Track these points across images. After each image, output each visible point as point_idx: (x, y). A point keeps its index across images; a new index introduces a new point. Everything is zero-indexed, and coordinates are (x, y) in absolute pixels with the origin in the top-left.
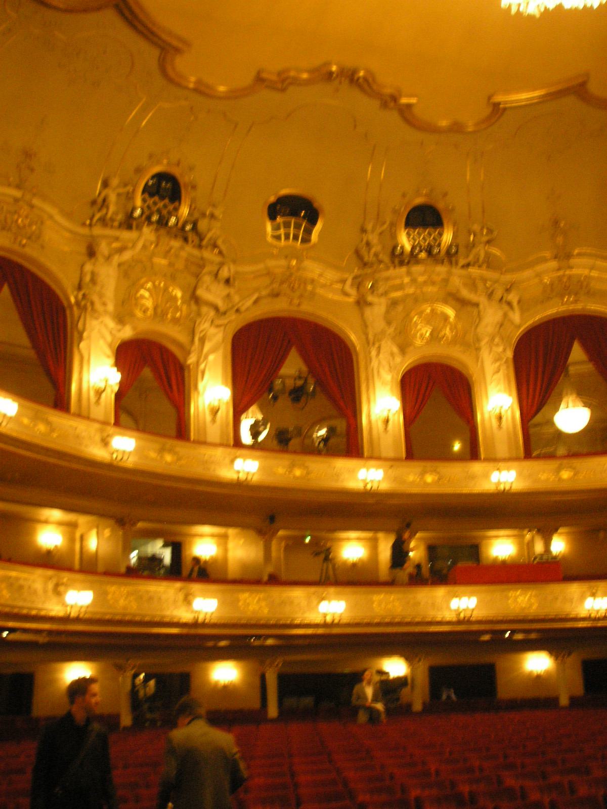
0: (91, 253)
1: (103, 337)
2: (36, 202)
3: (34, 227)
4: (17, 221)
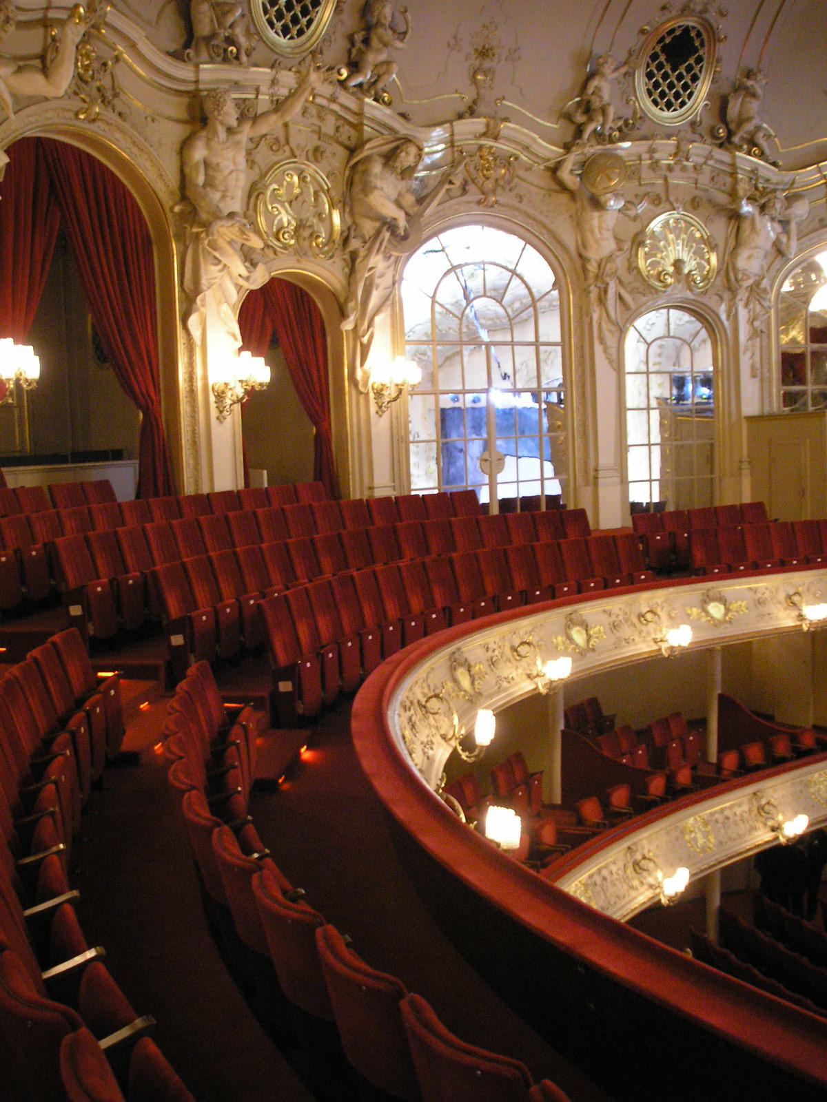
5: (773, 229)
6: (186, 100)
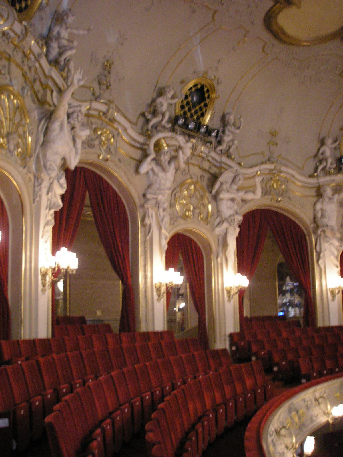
0: (319, 194)
1: (333, 254)
2: (283, 168)
3: (283, 187)
4: (273, 185)
6: (314, 190)
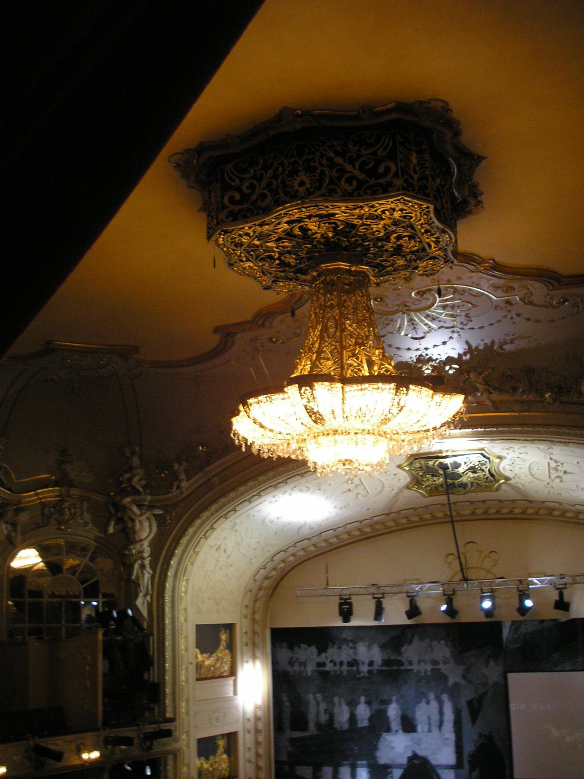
5: (7, 529)
